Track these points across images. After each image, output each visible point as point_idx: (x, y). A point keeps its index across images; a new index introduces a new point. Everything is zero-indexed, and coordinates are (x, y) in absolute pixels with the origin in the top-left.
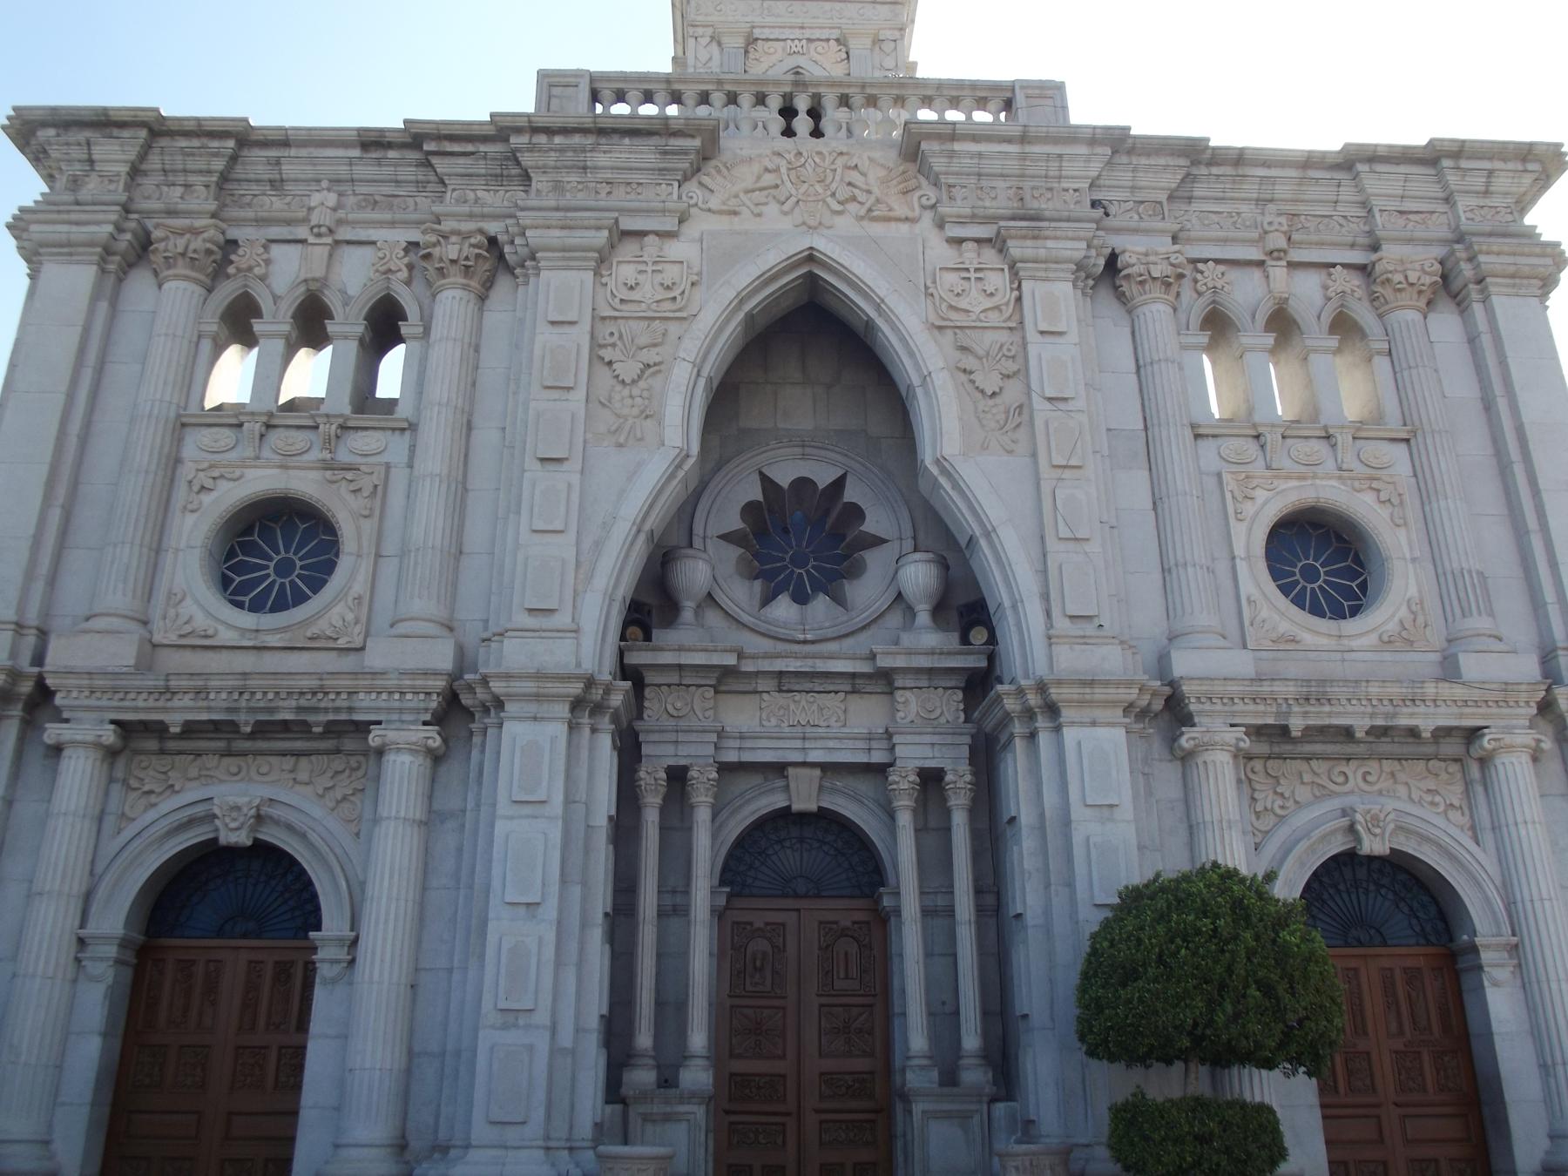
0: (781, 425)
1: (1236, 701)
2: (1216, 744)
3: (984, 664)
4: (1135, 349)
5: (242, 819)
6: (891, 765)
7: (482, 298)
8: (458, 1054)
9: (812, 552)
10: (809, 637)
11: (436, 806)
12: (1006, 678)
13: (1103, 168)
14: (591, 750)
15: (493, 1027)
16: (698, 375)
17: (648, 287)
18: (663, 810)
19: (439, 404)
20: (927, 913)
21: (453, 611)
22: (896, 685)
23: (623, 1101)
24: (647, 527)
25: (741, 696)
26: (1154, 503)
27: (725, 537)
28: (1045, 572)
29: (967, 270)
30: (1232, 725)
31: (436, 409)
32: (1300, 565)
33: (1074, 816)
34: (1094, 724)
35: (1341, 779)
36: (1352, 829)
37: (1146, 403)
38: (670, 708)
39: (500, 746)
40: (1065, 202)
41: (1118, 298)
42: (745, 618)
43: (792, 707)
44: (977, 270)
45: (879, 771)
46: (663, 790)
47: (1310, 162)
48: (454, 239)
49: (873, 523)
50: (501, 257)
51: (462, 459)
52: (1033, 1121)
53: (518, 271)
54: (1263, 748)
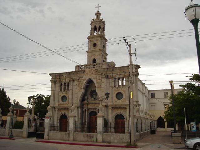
47: (121, 67)
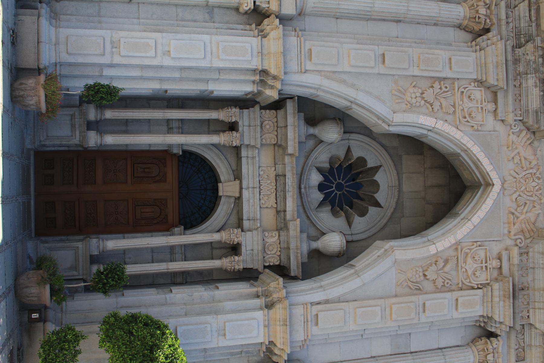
0: (404, 175)
3: (292, 274)
4: (450, 347)
6: (242, 231)
7: (459, 27)
8: (100, 22)
9: (343, 193)
10: (303, 190)
11: (216, 10)
12: (286, 285)
13: (540, 330)
14: (245, 82)
15: (112, 36)
16: (429, 130)
17: (471, 105)
18: (217, 121)
19: (408, 6)
20: (172, 249)
21: (309, 15)
22: (281, 232)
23: (81, 104)
24: (354, 106)
25: (273, 157)
26: (374, 357)
27: (349, 150)
28: (339, 301)
29: (486, 262)
31: (406, 4)
33: (219, 316)
37: (423, 353)
38: (267, 122)
39: (245, 36)
40: (522, 311)
41: (475, 339)
42: (310, 161)
43: (269, 182)
44: (486, 267)
45: (240, 225)
46: (226, 120)
48: (488, 11)
49: (359, 223)
50: (480, 35)
51: (384, 18)
52: (74, 299)
53: (474, 43)
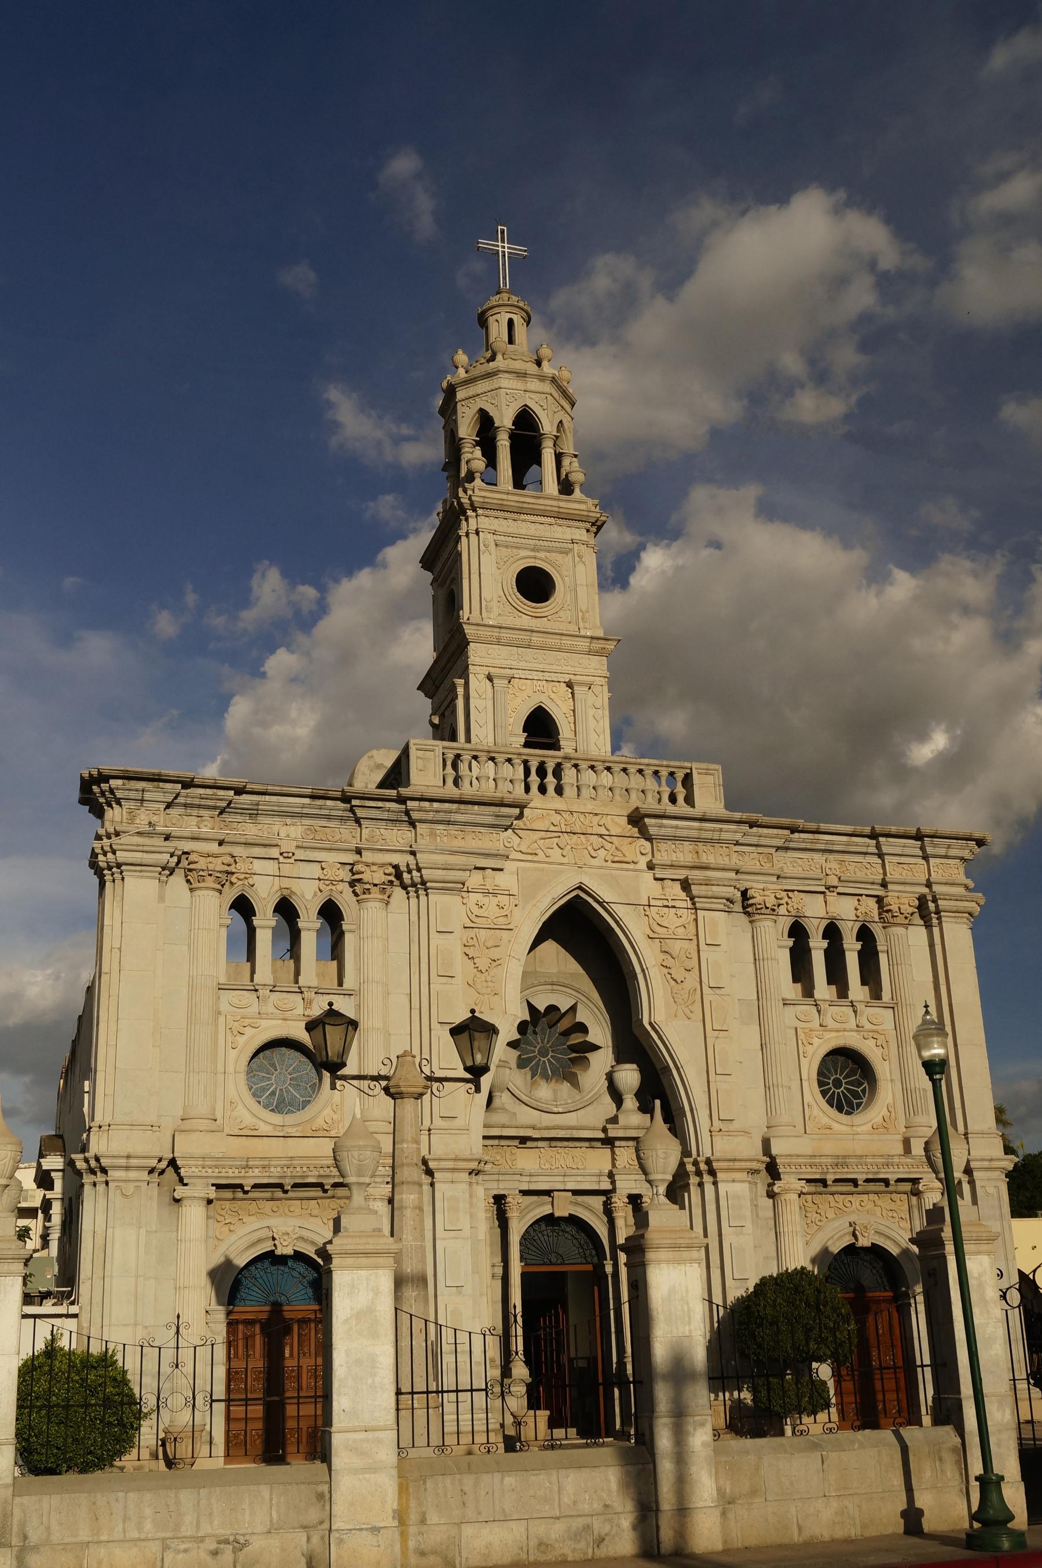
0: (538, 970)
1: (802, 1167)
2: (792, 1190)
5: (290, 1240)
10: (561, 1110)
30: (799, 1179)
32: (832, 1078)
34: (733, 1181)
35: (849, 1205)
36: (854, 1235)
42: (524, 1098)
43: (557, 1155)
54: (811, 1188)
